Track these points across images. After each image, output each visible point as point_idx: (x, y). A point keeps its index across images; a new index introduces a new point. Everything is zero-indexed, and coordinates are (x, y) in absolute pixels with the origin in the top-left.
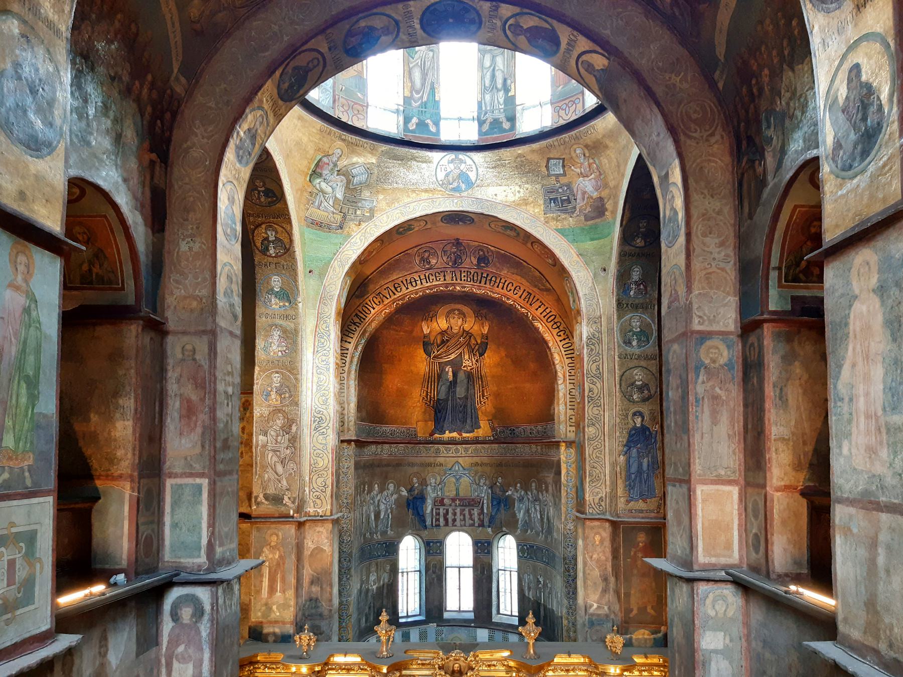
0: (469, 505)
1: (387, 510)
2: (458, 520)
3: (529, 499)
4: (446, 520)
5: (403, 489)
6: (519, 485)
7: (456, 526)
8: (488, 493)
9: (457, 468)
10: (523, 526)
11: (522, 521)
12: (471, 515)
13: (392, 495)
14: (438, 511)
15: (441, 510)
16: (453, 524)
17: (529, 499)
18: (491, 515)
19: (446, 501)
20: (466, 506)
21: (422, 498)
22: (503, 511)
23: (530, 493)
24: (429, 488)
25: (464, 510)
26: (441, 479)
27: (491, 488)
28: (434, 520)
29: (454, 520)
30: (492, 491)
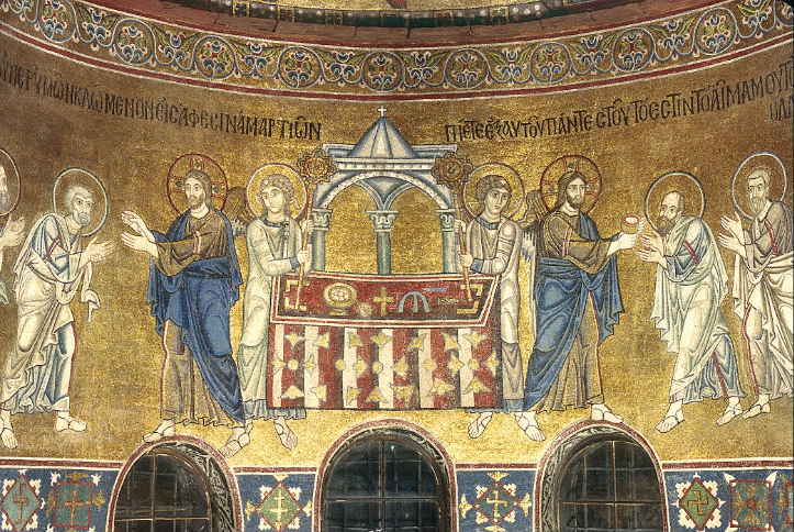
0: (436, 312)
1: (54, 307)
2: (385, 379)
3: (729, 256)
4: (332, 380)
5: (138, 223)
6: (672, 199)
7: (375, 407)
8: (523, 253)
9: (381, 149)
10: (699, 384)
11: (692, 363)
12: (442, 356)
13: (82, 239)
14: (294, 339)
15: (311, 333)
16: (361, 399)
17: (729, 256)
18: (536, 353)
19: (338, 295)
20: (421, 315)
21: (223, 271)
22: (592, 331)
23: (735, 226)
24: (256, 231)
25: (412, 333)
26: (311, 194)
27: (536, 228)
28: (278, 378)
29: (368, 382)
30: (539, 244)
